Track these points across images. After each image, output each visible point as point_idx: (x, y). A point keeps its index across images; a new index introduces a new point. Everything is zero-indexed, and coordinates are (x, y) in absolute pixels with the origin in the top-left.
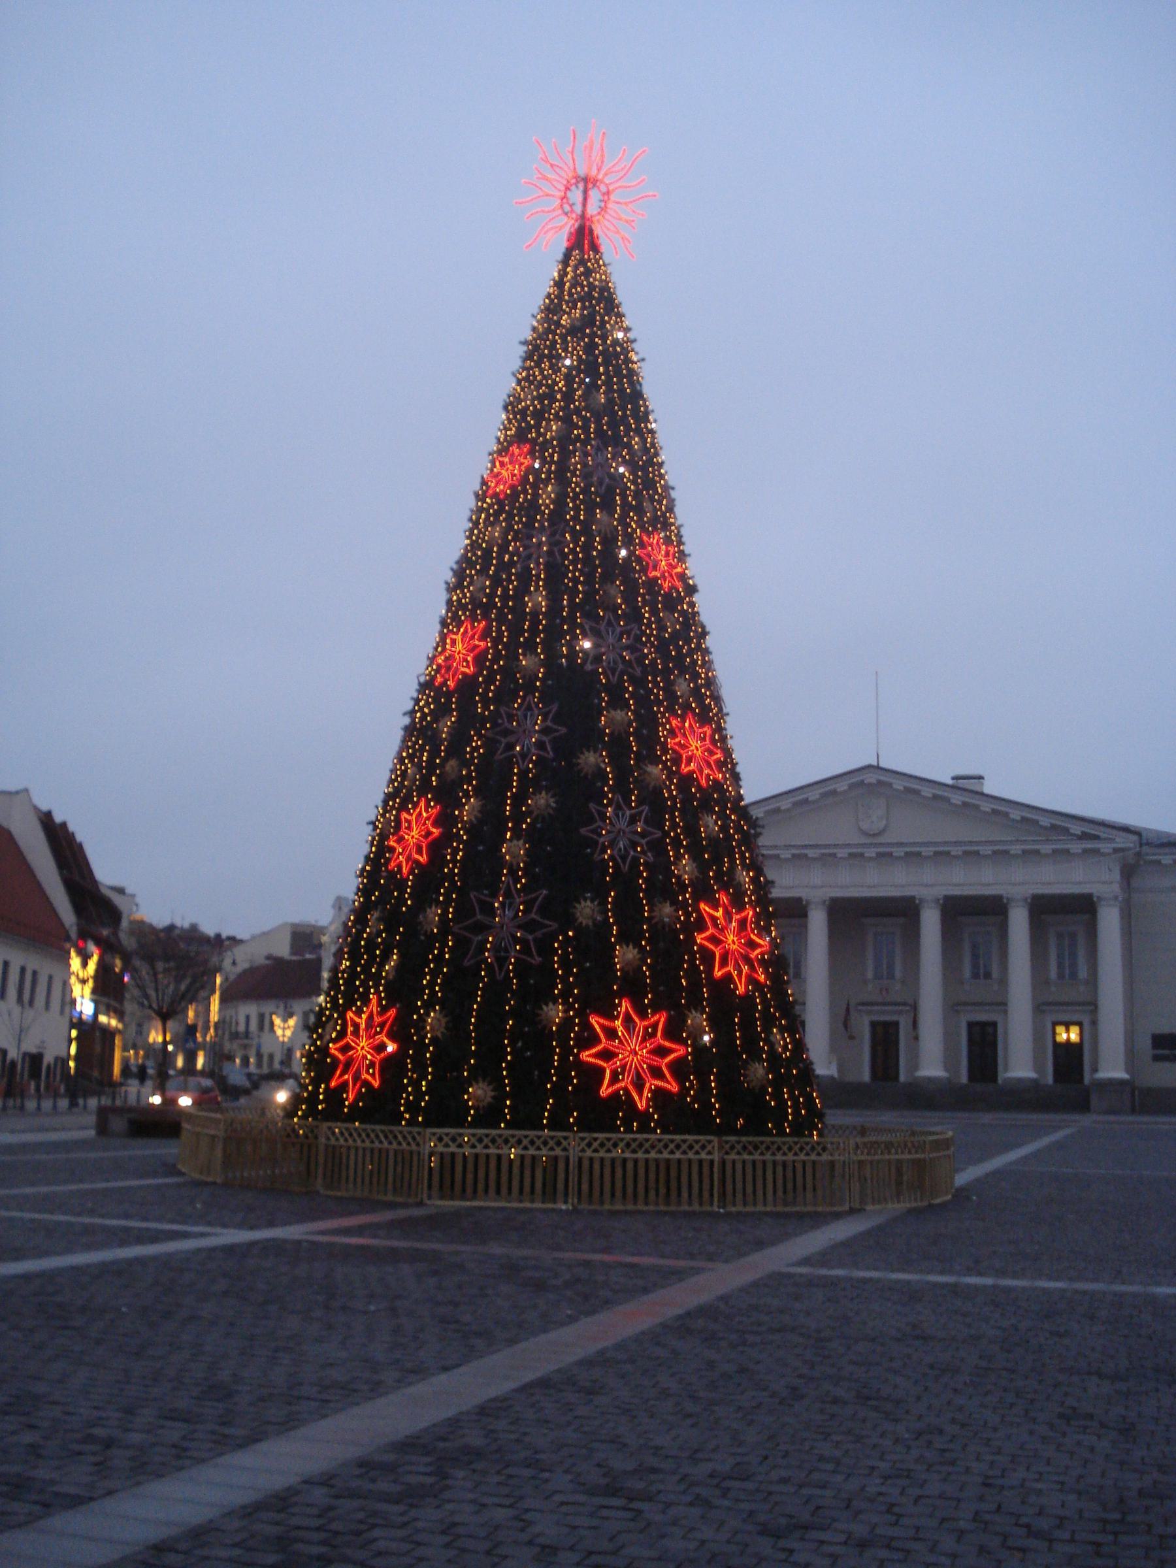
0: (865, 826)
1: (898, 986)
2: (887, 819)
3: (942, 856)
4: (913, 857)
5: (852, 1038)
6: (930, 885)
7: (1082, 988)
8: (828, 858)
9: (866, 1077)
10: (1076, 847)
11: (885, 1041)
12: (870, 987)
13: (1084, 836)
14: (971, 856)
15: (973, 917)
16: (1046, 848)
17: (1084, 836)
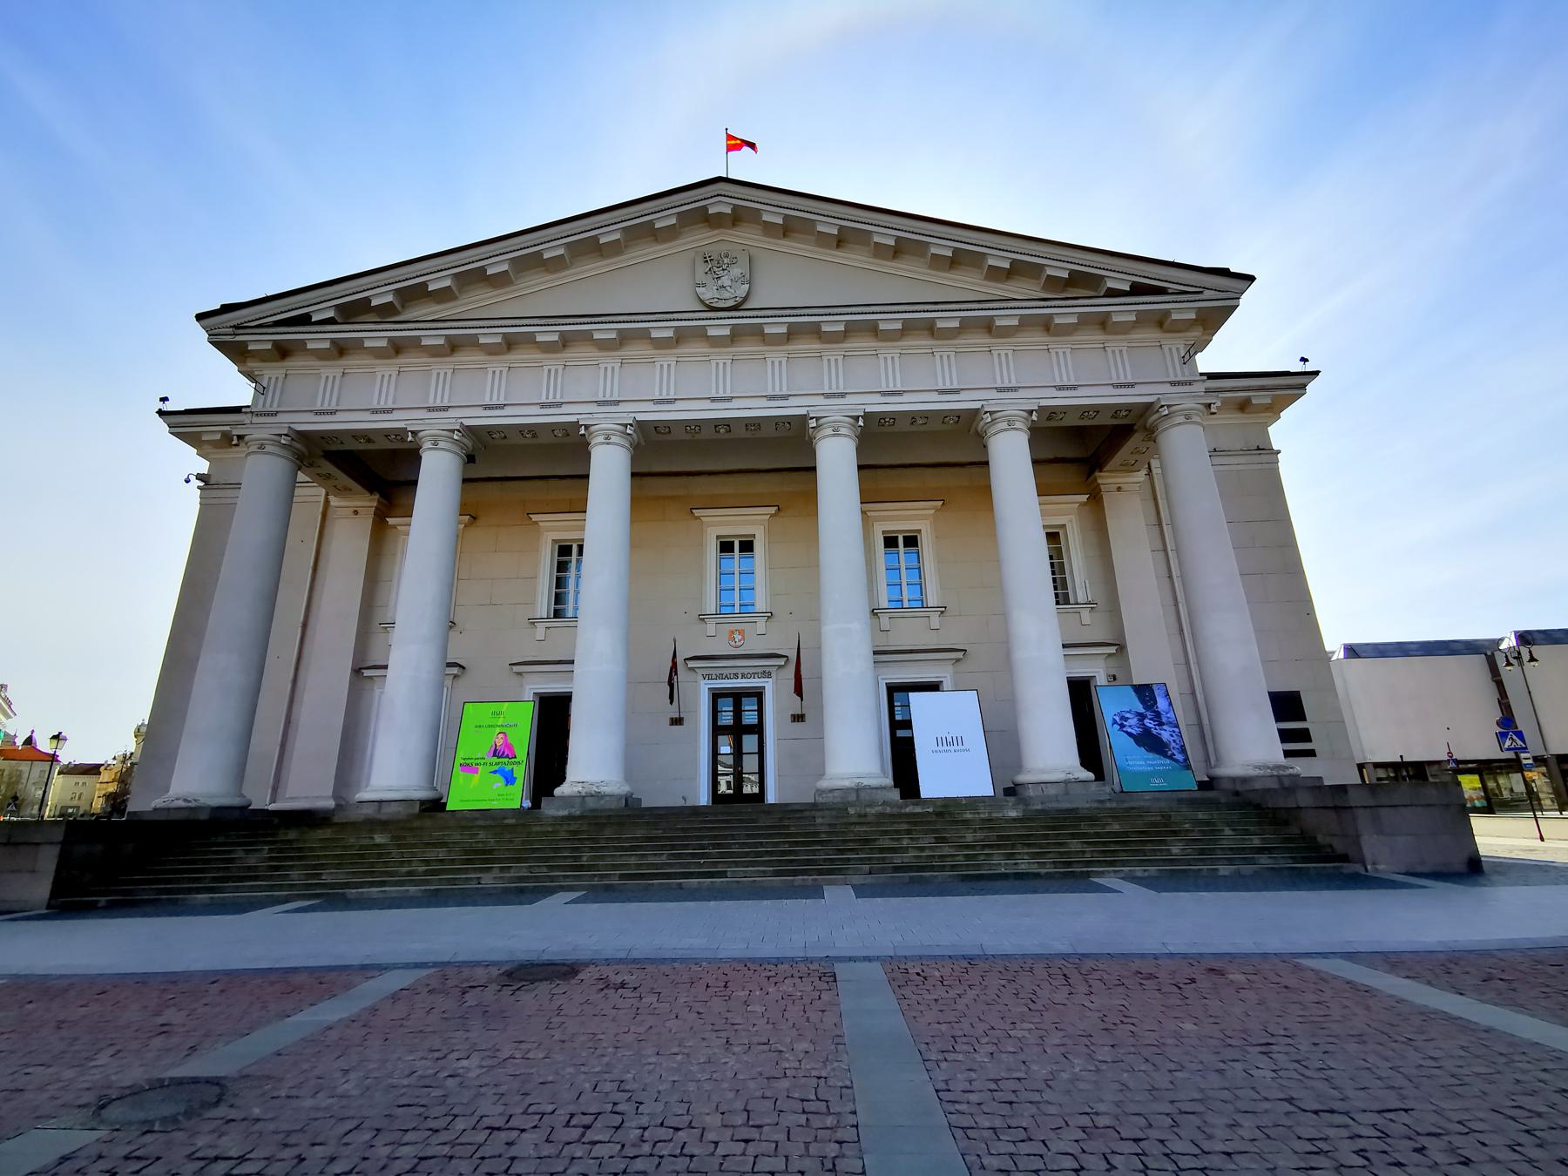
0: (708, 294)
1: (761, 625)
2: (750, 283)
3: (863, 328)
4: (804, 330)
5: (677, 721)
6: (834, 392)
7: (1086, 616)
8: (630, 335)
9: (704, 799)
10: (1124, 312)
11: (737, 721)
12: (711, 628)
13: (1138, 290)
14: (921, 327)
15: (923, 460)
16: (1065, 315)
17: (1138, 290)
